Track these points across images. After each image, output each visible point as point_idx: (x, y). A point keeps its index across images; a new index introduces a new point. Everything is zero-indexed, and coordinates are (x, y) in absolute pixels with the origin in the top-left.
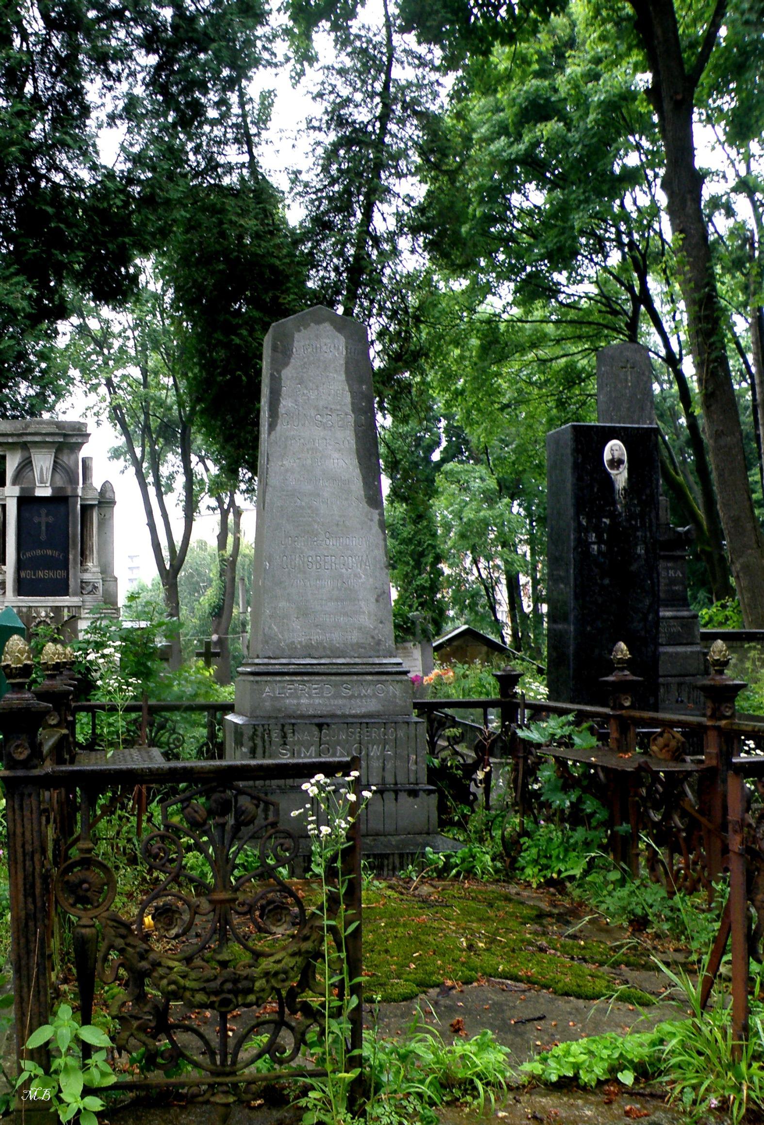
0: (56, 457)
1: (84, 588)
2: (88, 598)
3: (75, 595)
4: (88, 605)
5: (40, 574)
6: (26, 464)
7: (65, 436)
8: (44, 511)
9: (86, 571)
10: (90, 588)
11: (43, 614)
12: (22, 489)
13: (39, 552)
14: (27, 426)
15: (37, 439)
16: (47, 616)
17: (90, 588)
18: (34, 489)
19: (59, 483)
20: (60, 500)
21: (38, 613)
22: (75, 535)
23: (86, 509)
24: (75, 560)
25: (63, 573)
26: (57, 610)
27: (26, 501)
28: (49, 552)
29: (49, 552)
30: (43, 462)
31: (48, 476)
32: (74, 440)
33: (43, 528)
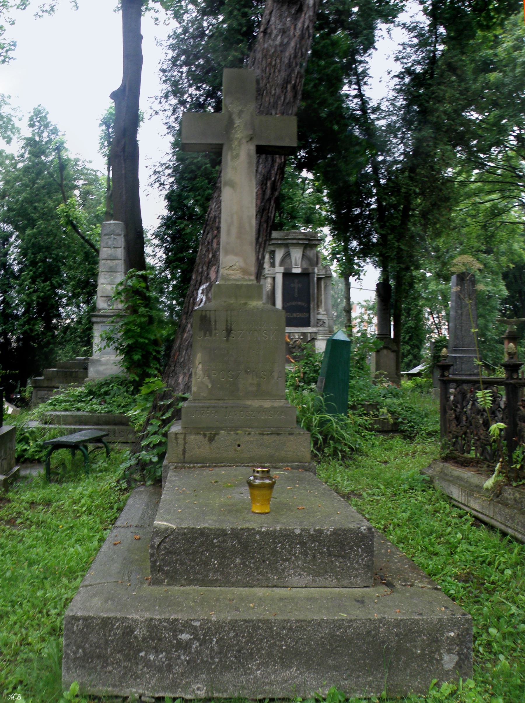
0: (303, 252)
1: (319, 323)
2: (321, 328)
3: (314, 326)
4: (321, 332)
5: (295, 315)
6: (287, 255)
7: (309, 240)
8: (296, 281)
9: (318, 313)
10: (321, 323)
11: (297, 337)
12: (285, 269)
13: (294, 303)
14: (287, 235)
15: (295, 241)
16: (299, 338)
17: (321, 323)
18: (291, 269)
19: (305, 266)
20: (306, 275)
21: (294, 336)
22: (314, 294)
23: (319, 279)
24: (314, 308)
25: (307, 315)
26: (304, 334)
27: (287, 275)
28: (300, 303)
29: (300, 303)
30: (296, 254)
31: (299, 261)
32: (313, 243)
33: (296, 290)
